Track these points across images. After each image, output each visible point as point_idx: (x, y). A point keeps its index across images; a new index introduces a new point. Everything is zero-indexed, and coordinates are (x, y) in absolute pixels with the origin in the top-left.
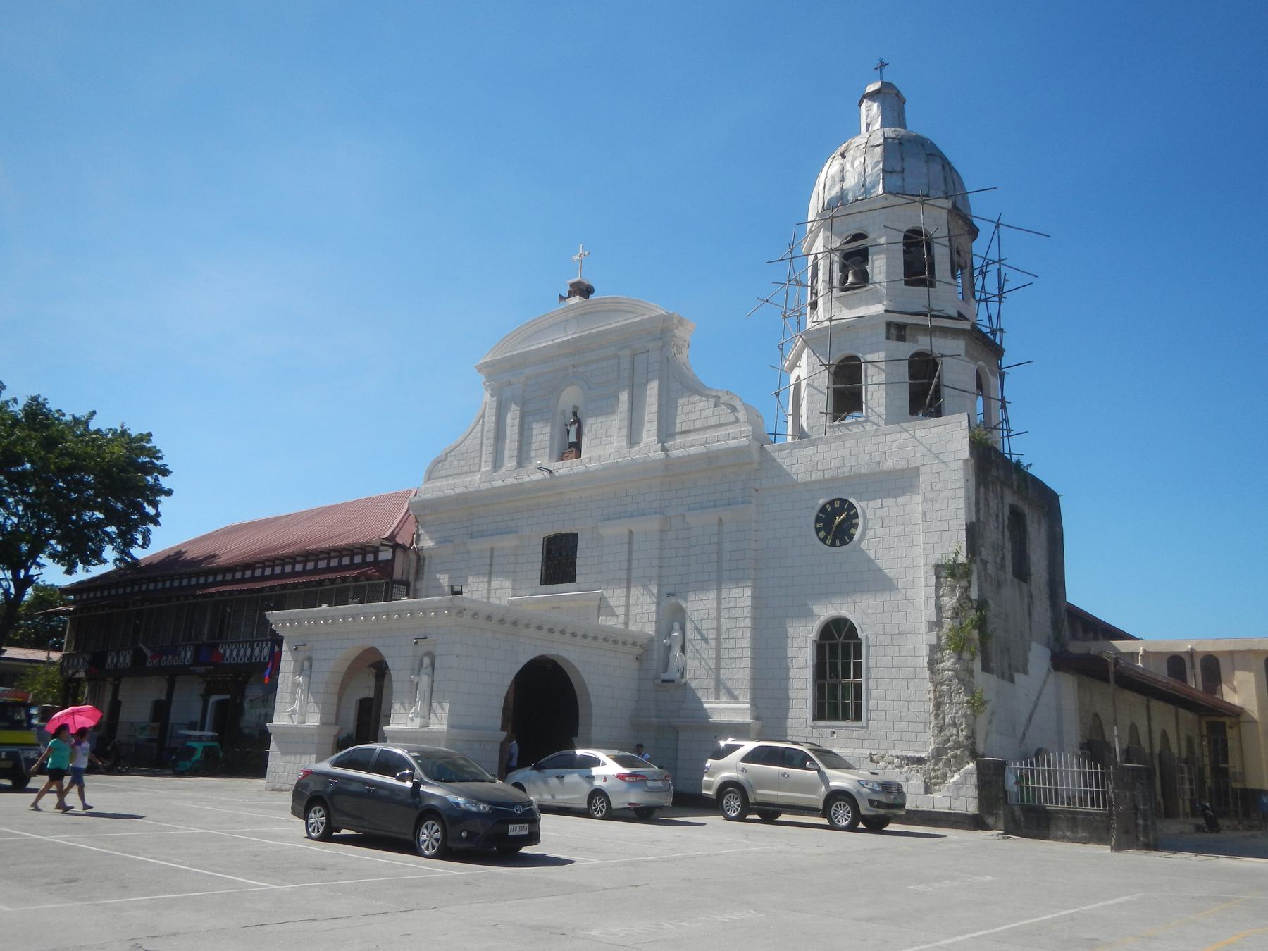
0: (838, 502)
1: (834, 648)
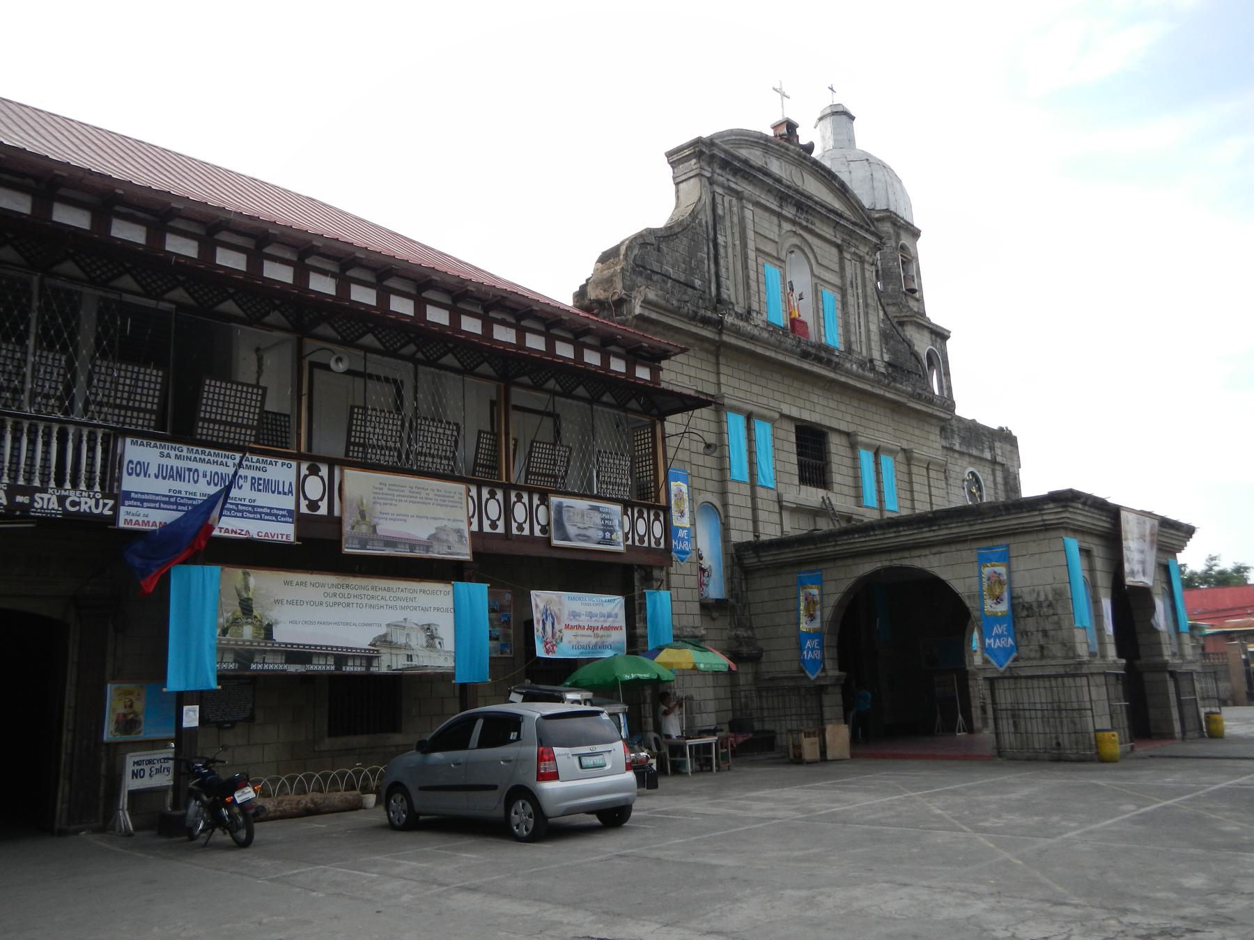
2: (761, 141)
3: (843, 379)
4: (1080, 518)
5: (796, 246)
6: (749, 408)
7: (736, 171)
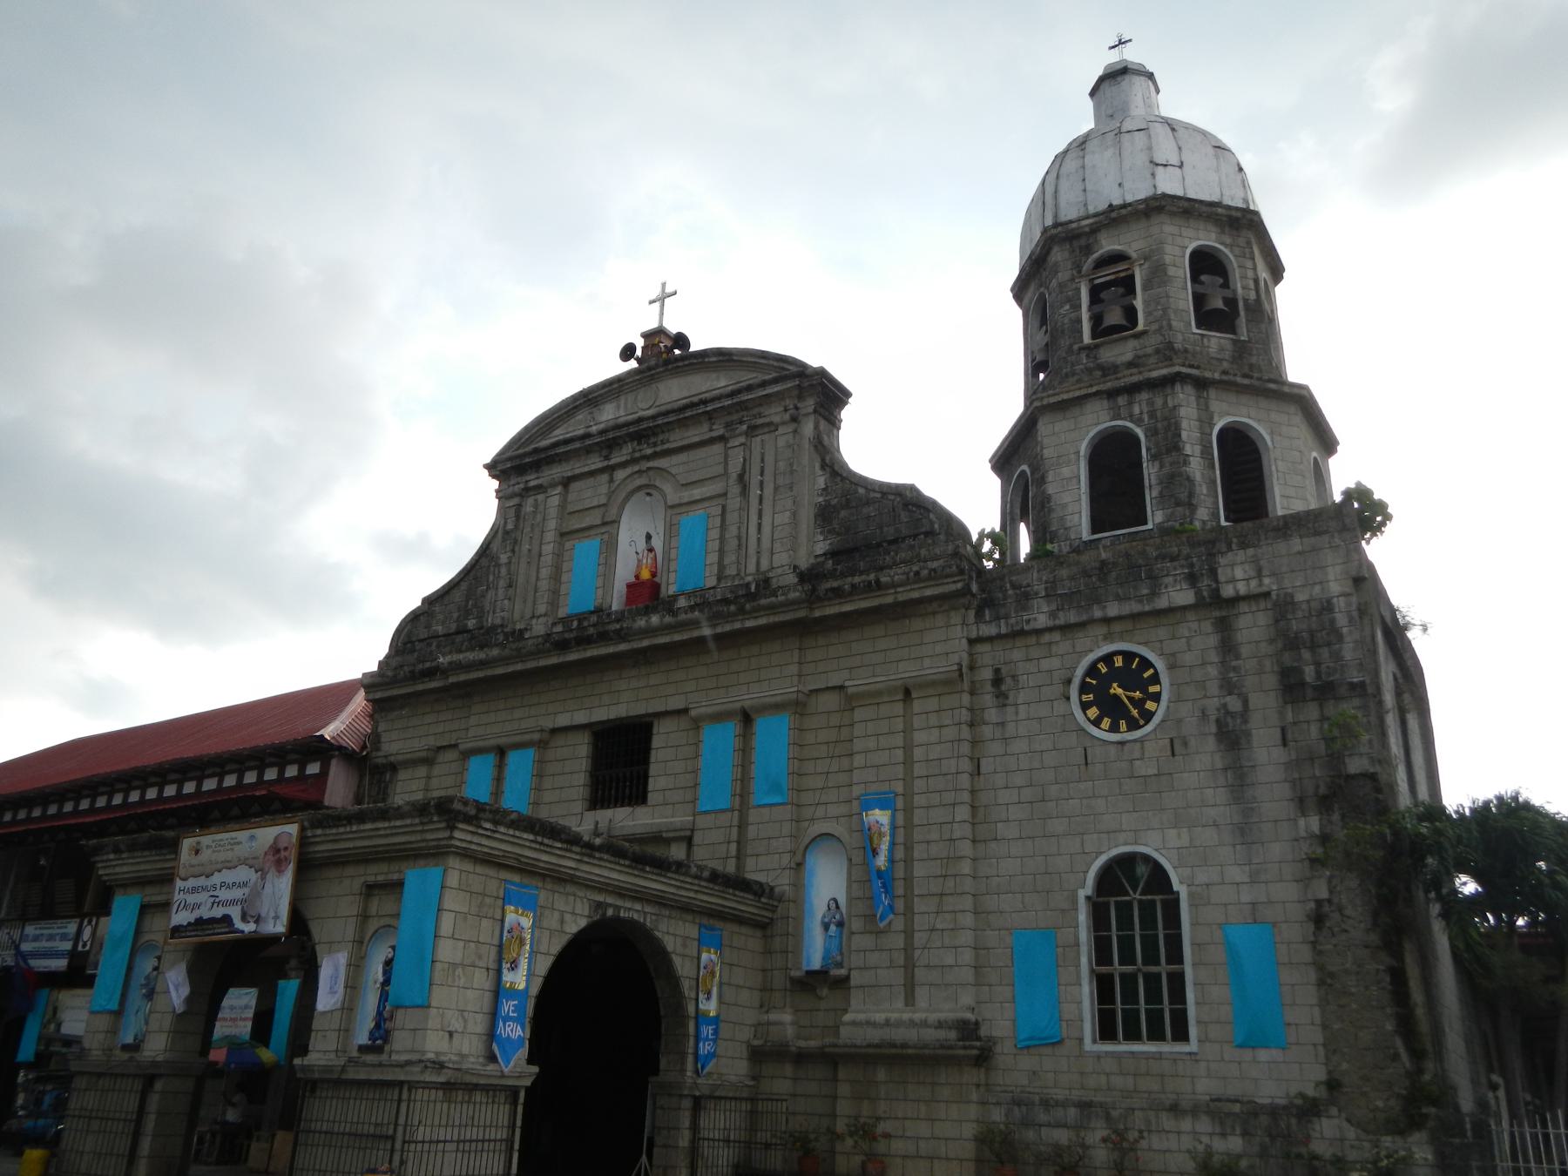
0: (1120, 658)
1: (1124, 910)
2: (578, 403)
3: (645, 643)
4: (125, 869)
5: (639, 488)
6: (492, 742)
7: (537, 466)
